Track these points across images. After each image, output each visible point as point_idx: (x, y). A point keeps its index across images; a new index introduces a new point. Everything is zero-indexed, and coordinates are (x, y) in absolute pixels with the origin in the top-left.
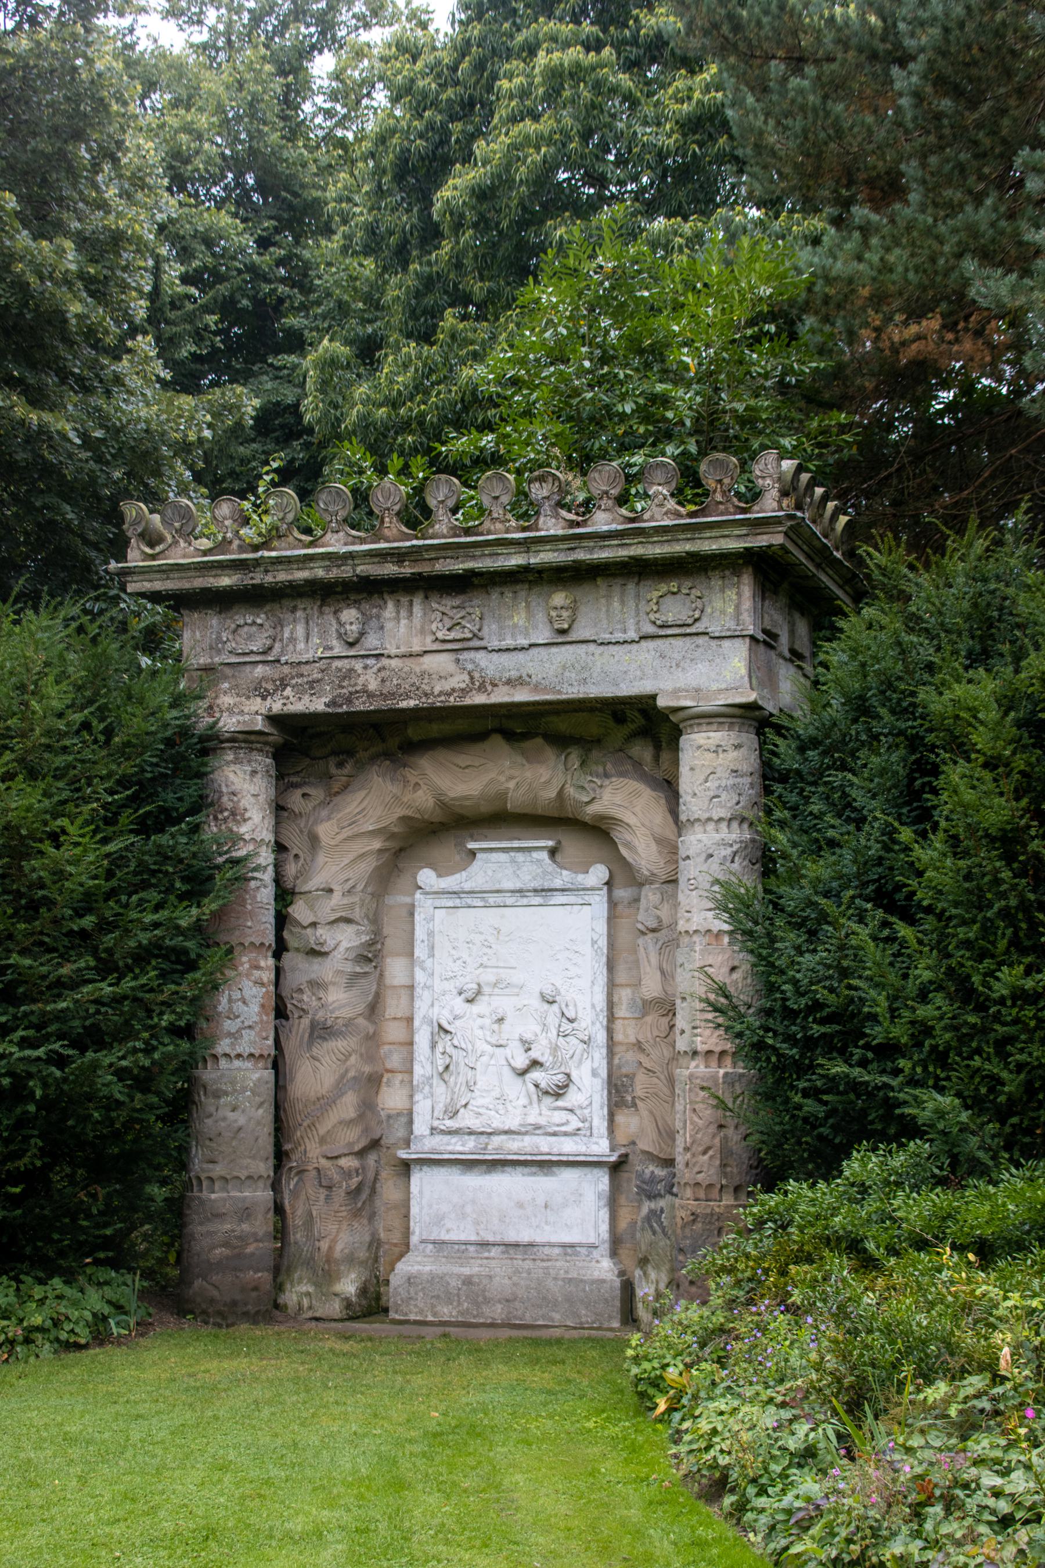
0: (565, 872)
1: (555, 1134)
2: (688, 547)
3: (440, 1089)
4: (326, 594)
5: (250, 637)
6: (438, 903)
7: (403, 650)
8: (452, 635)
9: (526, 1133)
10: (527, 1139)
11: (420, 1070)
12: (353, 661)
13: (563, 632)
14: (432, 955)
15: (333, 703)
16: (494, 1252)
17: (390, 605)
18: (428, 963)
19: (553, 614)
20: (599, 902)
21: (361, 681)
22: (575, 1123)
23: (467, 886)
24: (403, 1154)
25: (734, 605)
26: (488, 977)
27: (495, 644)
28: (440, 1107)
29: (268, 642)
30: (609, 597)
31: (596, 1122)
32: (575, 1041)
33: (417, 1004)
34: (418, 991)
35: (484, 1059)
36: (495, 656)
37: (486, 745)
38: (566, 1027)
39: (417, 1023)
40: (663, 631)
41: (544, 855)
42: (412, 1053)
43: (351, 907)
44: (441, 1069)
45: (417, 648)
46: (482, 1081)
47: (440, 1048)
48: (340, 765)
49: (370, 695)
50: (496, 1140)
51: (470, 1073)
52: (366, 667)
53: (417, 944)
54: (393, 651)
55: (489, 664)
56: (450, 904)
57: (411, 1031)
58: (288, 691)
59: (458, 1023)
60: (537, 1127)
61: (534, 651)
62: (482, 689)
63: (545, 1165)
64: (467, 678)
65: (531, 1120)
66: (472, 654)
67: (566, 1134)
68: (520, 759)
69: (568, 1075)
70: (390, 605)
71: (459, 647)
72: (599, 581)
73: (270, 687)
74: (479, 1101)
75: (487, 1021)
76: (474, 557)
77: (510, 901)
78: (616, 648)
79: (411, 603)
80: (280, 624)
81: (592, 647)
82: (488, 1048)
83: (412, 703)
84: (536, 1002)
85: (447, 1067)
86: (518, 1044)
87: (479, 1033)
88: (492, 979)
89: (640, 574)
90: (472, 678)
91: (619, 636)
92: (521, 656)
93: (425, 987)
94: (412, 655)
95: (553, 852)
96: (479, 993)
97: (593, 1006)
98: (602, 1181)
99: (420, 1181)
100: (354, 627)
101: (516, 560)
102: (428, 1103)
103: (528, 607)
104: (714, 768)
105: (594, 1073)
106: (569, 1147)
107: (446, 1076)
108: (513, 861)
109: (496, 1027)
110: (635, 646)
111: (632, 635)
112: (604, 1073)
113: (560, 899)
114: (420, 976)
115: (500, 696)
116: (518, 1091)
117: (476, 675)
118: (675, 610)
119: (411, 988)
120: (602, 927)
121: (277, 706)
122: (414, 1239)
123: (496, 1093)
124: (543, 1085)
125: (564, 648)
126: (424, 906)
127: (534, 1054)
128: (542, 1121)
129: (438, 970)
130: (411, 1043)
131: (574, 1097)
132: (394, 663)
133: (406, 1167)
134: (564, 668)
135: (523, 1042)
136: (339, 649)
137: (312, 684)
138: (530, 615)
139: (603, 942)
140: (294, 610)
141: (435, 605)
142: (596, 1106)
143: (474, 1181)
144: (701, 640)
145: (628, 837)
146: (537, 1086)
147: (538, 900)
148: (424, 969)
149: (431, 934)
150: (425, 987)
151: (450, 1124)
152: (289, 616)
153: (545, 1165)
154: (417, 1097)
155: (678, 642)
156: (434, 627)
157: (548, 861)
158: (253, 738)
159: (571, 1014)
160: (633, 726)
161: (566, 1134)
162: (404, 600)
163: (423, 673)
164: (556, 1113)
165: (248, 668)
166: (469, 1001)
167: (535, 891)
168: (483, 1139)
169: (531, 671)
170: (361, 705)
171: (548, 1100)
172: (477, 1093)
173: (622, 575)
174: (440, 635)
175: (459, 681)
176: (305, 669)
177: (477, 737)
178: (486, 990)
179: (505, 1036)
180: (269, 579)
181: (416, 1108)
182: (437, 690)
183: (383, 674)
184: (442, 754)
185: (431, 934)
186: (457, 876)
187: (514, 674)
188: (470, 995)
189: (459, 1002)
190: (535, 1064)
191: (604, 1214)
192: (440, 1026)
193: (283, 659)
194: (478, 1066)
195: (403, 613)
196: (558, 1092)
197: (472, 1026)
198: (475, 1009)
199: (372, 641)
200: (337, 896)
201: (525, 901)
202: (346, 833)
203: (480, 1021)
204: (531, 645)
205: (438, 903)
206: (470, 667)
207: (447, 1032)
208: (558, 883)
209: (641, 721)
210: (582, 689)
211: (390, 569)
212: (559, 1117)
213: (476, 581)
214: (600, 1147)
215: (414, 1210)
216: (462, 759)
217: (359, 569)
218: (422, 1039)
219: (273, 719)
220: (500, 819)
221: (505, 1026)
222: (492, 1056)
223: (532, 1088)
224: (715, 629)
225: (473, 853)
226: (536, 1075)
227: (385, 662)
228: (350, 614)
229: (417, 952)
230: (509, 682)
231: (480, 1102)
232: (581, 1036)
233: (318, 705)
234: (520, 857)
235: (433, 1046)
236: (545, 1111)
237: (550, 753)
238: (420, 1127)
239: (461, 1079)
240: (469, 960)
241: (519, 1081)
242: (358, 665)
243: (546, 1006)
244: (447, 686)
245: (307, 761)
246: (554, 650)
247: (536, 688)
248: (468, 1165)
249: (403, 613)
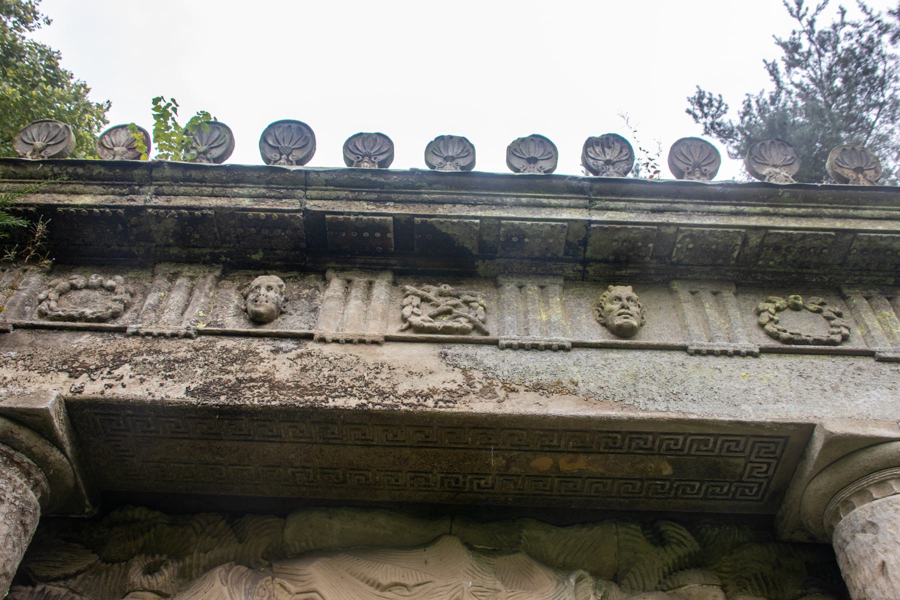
2: (839, 224)
5: (85, 303)
7: (349, 332)
8: (437, 324)
12: (255, 343)
15: (204, 391)
19: (616, 306)
21: (262, 368)
27: (511, 336)
29: (118, 306)
36: (511, 355)
37: (430, 553)
48: (150, 570)
49: (275, 386)
52: (276, 351)
54: (330, 333)
58: (125, 370)
61: (580, 354)
62: (487, 392)
64: (459, 378)
66: (470, 350)
68: (491, 581)
70: (336, 285)
72: (676, 285)
73: (93, 362)
76: (501, 205)
78: (721, 362)
79: (370, 284)
81: (679, 357)
83: (353, 403)
89: (738, 285)
90: (469, 380)
92: (557, 358)
100: (272, 294)
103: (563, 304)
110: (752, 362)
115: (523, 405)
117: (477, 375)
118: (806, 325)
121: (93, 388)
125: (631, 355)
132: (328, 350)
134: (635, 377)
137: (170, 365)
138: (569, 315)
140: (176, 275)
141: (410, 288)
144: (862, 362)
152: (161, 281)
155: (825, 362)
156: (407, 311)
158: (24, 435)
160: (681, 551)
162: (360, 281)
163: (378, 368)
165: (64, 336)
169: (578, 378)
170: (251, 398)
173: (710, 281)
174: (415, 320)
176: (164, 345)
180: (161, 201)
182: (402, 389)
183: (305, 361)
187: (546, 378)
193: (132, 328)
195: (356, 292)
204: (576, 345)
206: (465, 363)
209: (691, 545)
210: (672, 405)
213: (481, 267)
217: (310, 205)
219: (74, 408)
227: (311, 346)
230: (537, 388)
233: (175, 392)
237: (543, 575)
242: (264, 348)
244: (422, 386)
245: (93, 559)
246: (613, 355)
247: (588, 398)
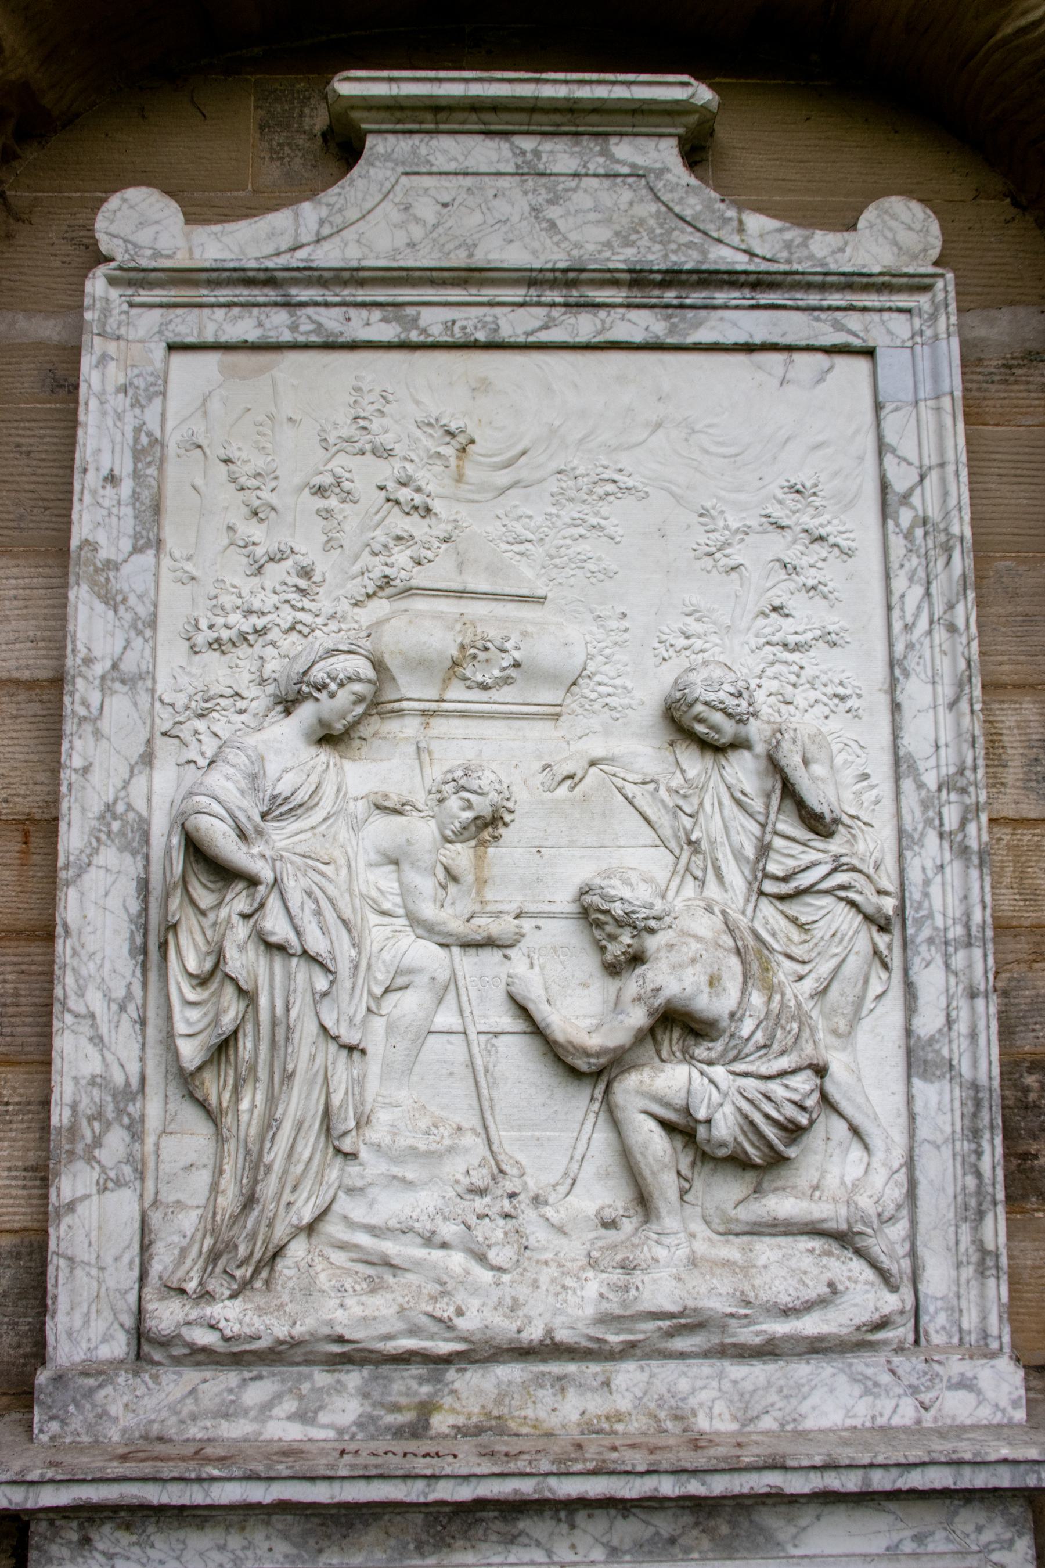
0: (756, 222)
1: (768, 1351)
3: (184, 1145)
6: (187, 325)
9: (629, 1350)
10: (628, 1375)
14: (149, 540)
18: (134, 576)
22: (865, 1299)
26: (424, 631)
28: (182, 1227)
31: (938, 1278)
32: (846, 920)
33: (78, 749)
34: (83, 693)
35: (408, 1004)
38: (795, 853)
39: (72, 839)
41: (663, 154)
42: (47, 976)
44: (190, 1052)
46: (399, 1104)
47: (190, 954)
50: (474, 1391)
51: (342, 1071)
53: (87, 484)
56: (244, 327)
57: (45, 877)
59: (282, 836)
60: (688, 1322)
65: (660, 1291)
67: (817, 1347)
69: (820, 1071)
74: (388, 1204)
75: (422, 831)
77: (515, 324)
82: (425, 953)
84: (643, 752)
85: (224, 1048)
86: (565, 933)
87: (385, 880)
88: (443, 642)
93: (117, 676)
96: (377, 705)
97: (901, 765)
102: (124, 1206)
105: (917, 1059)
107: (214, 1087)
108: (529, 172)
109: (461, 855)
112: (985, 1064)
114: (93, 629)
116: (559, 1146)
120: (932, 437)
123: (468, 1162)
124: (725, 1128)
127: (674, 975)
128: (714, 1296)
129: (176, 606)
130: (45, 933)
131: (836, 1176)
135: (593, 916)
142: (937, 1204)
146: (682, 1128)
148: (111, 599)
149: (148, 450)
150: (117, 676)
151: (234, 1316)
154: (72, 1183)
157: (679, 172)
159: (818, 795)
161: (817, 1347)
164: (767, 1251)
166: (330, 738)
167: (638, 279)
168: (407, 1385)
171: (727, 1192)
172: (372, 1166)
178: (412, 689)
179: (505, 896)
181: (68, 1237)
185: (148, 450)
186: (281, 219)
188: (337, 705)
189: (284, 746)
190: (678, 1025)
192: (197, 852)
194: (376, 1041)
197: (346, 845)
198: (360, 775)
201: (584, 326)
203: (383, 829)
205: (187, 325)
207: (224, 874)
212: (785, 1269)
218: (97, 912)
221: (509, 853)
222: (446, 989)
223: (654, 1144)
226: (672, 1078)
229: (85, 524)
231: (391, 1206)
232: (869, 899)
234: (560, 155)
235: (152, 945)
236: (707, 1245)
238: (84, 1327)
239: (299, 1103)
240: (324, 566)
241: (577, 1105)
243: (694, 764)
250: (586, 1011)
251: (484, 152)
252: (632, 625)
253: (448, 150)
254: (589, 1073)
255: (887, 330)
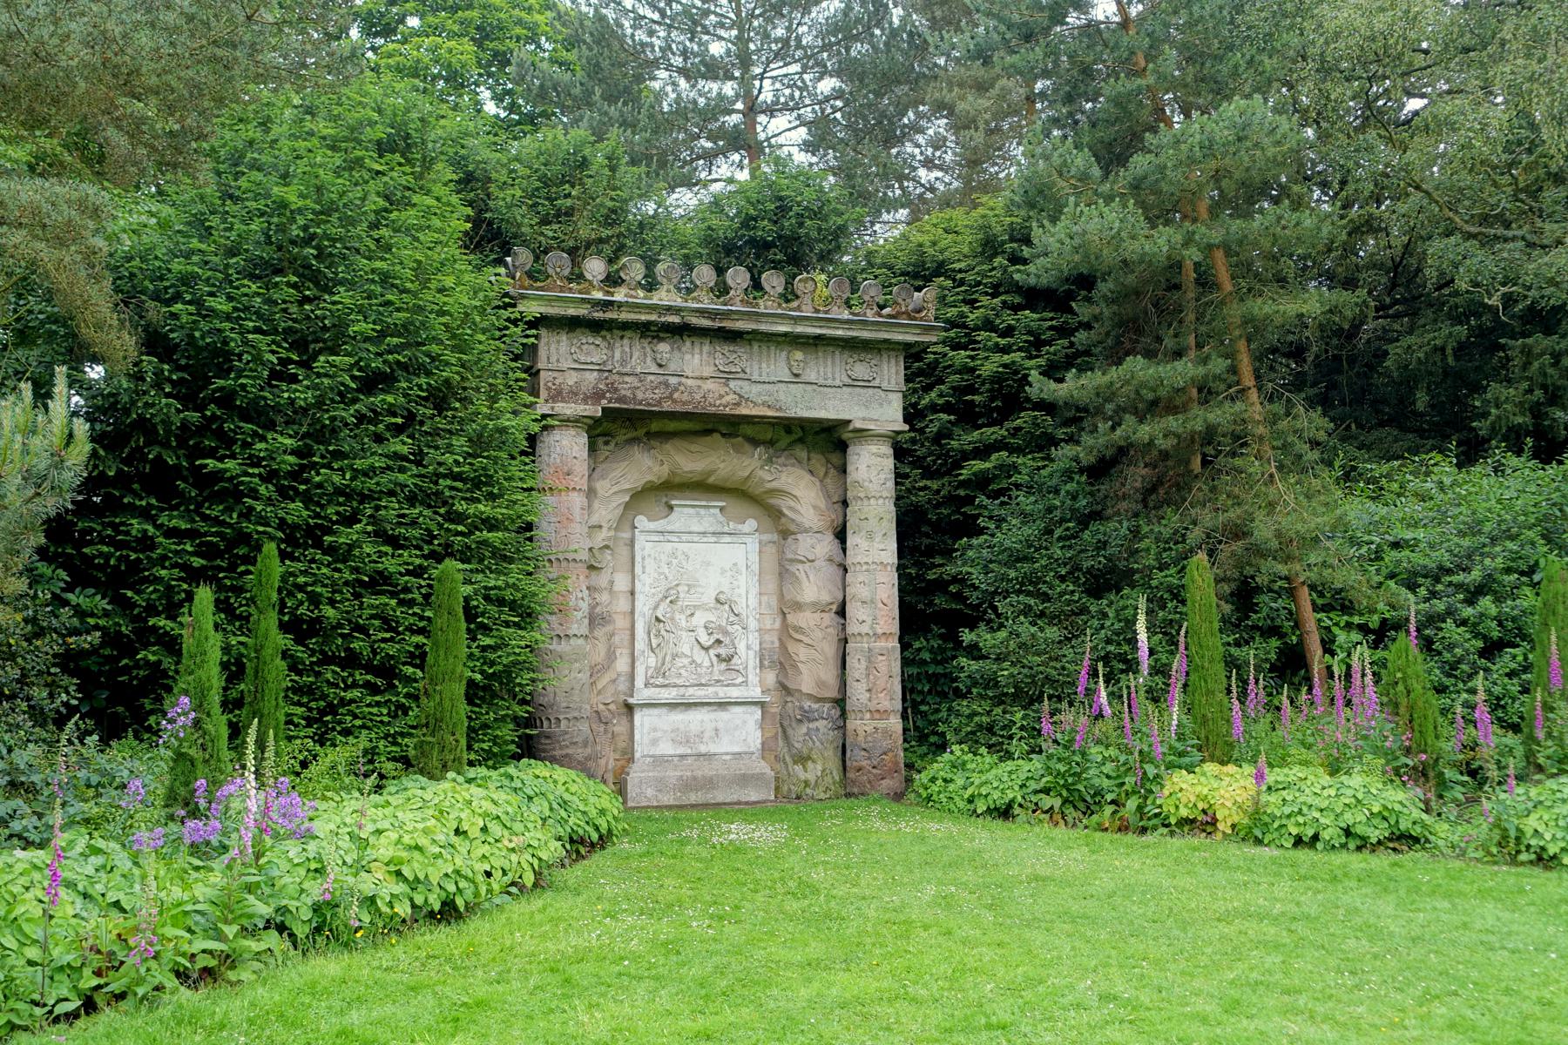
4: (649, 331)
7: (697, 374)
10: (711, 689)
11: (640, 645)
13: (797, 375)
16: (690, 760)
17: (688, 344)
20: (753, 544)
23: (669, 528)
24: (631, 701)
25: (892, 373)
27: (755, 377)
30: (825, 358)
31: (750, 677)
40: (854, 383)
43: (609, 539)
45: (705, 374)
48: (606, 443)
55: (752, 391)
63: (723, 705)
66: (740, 383)
70: (688, 344)
71: (726, 377)
80: (611, 347)
91: (829, 382)
94: (697, 376)
95: (722, 509)
98: (758, 713)
99: (638, 717)
101: (783, 328)
104: (872, 469)
105: (748, 647)
106: (735, 693)
111: (838, 383)
113: (727, 539)
118: (861, 370)
119: (632, 593)
120: (754, 558)
122: (637, 755)
126: (640, 540)
132: (689, 382)
133: (630, 709)
136: (654, 369)
139: (756, 567)
140: (622, 338)
143: (678, 717)
145: (792, 504)
146: (718, 656)
147: (713, 539)
153: (723, 705)
154: (637, 664)
175: (731, 398)
177: (707, 432)
184: (677, 442)
190: (719, 642)
191: (759, 733)
195: (697, 350)
196: (729, 659)
199: (672, 367)
200: (604, 530)
202: (615, 489)
208: (726, 529)
209: (800, 434)
211: (706, 323)
214: (755, 693)
215: (637, 737)
216: (693, 447)
220: (702, 487)
223: (715, 659)
224: (885, 385)
225: (671, 508)
227: (683, 380)
228: (663, 347)
234: (702, 511)
244: (724, 401)
248: (673, 706)
249: (697, 350)
250: (706, 640)
251: (691, 511)
252: (711, 583)
253: (686, 510)
254: (706, 649)
255: (748, 540)
